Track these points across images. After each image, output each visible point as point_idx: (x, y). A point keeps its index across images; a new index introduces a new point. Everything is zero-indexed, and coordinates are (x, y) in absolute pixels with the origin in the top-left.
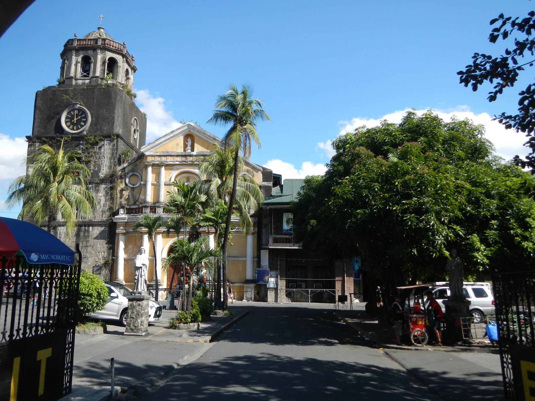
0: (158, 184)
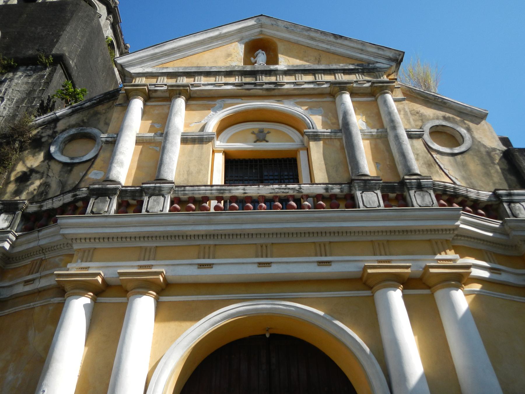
0: (159, 139)
